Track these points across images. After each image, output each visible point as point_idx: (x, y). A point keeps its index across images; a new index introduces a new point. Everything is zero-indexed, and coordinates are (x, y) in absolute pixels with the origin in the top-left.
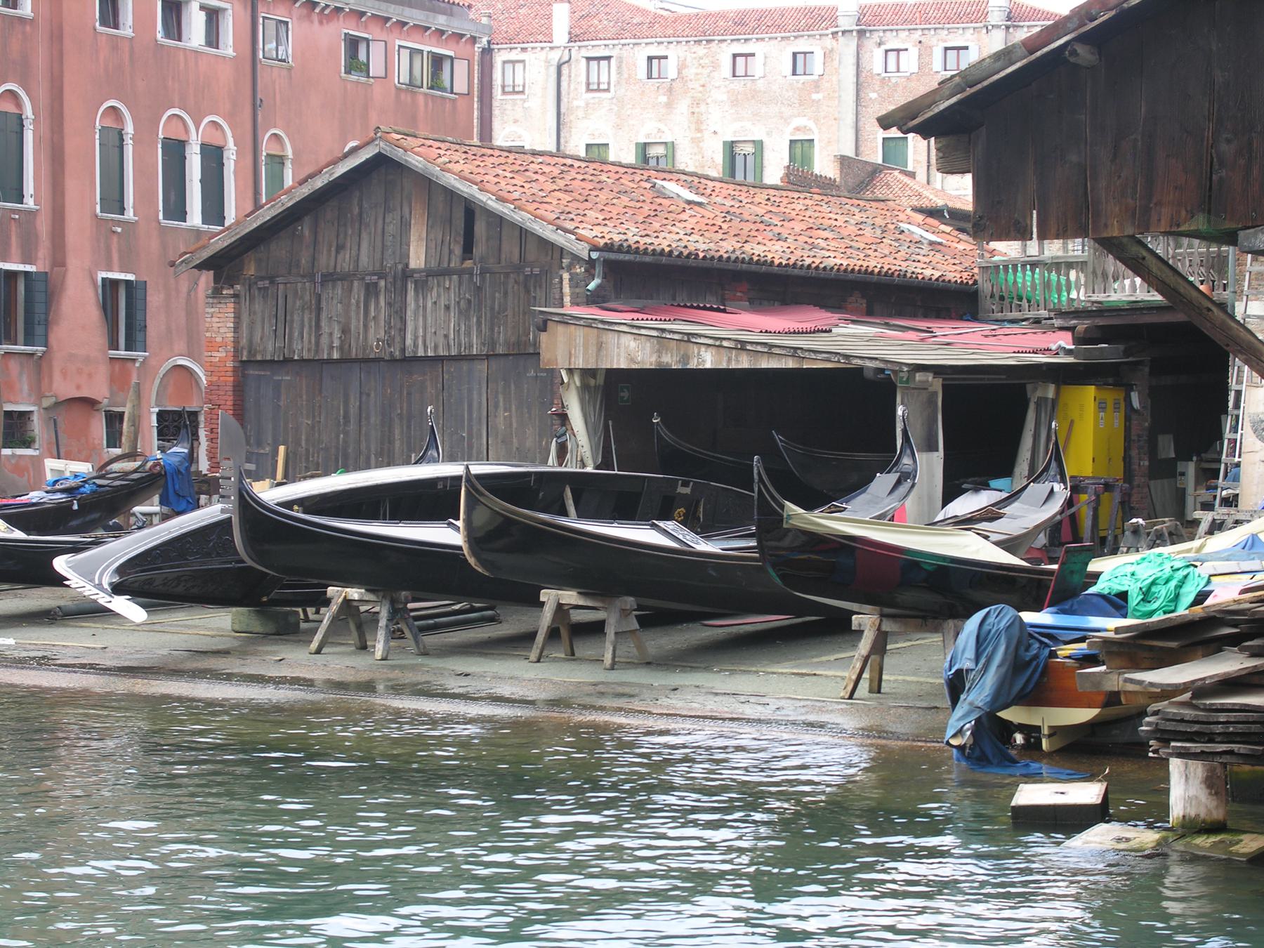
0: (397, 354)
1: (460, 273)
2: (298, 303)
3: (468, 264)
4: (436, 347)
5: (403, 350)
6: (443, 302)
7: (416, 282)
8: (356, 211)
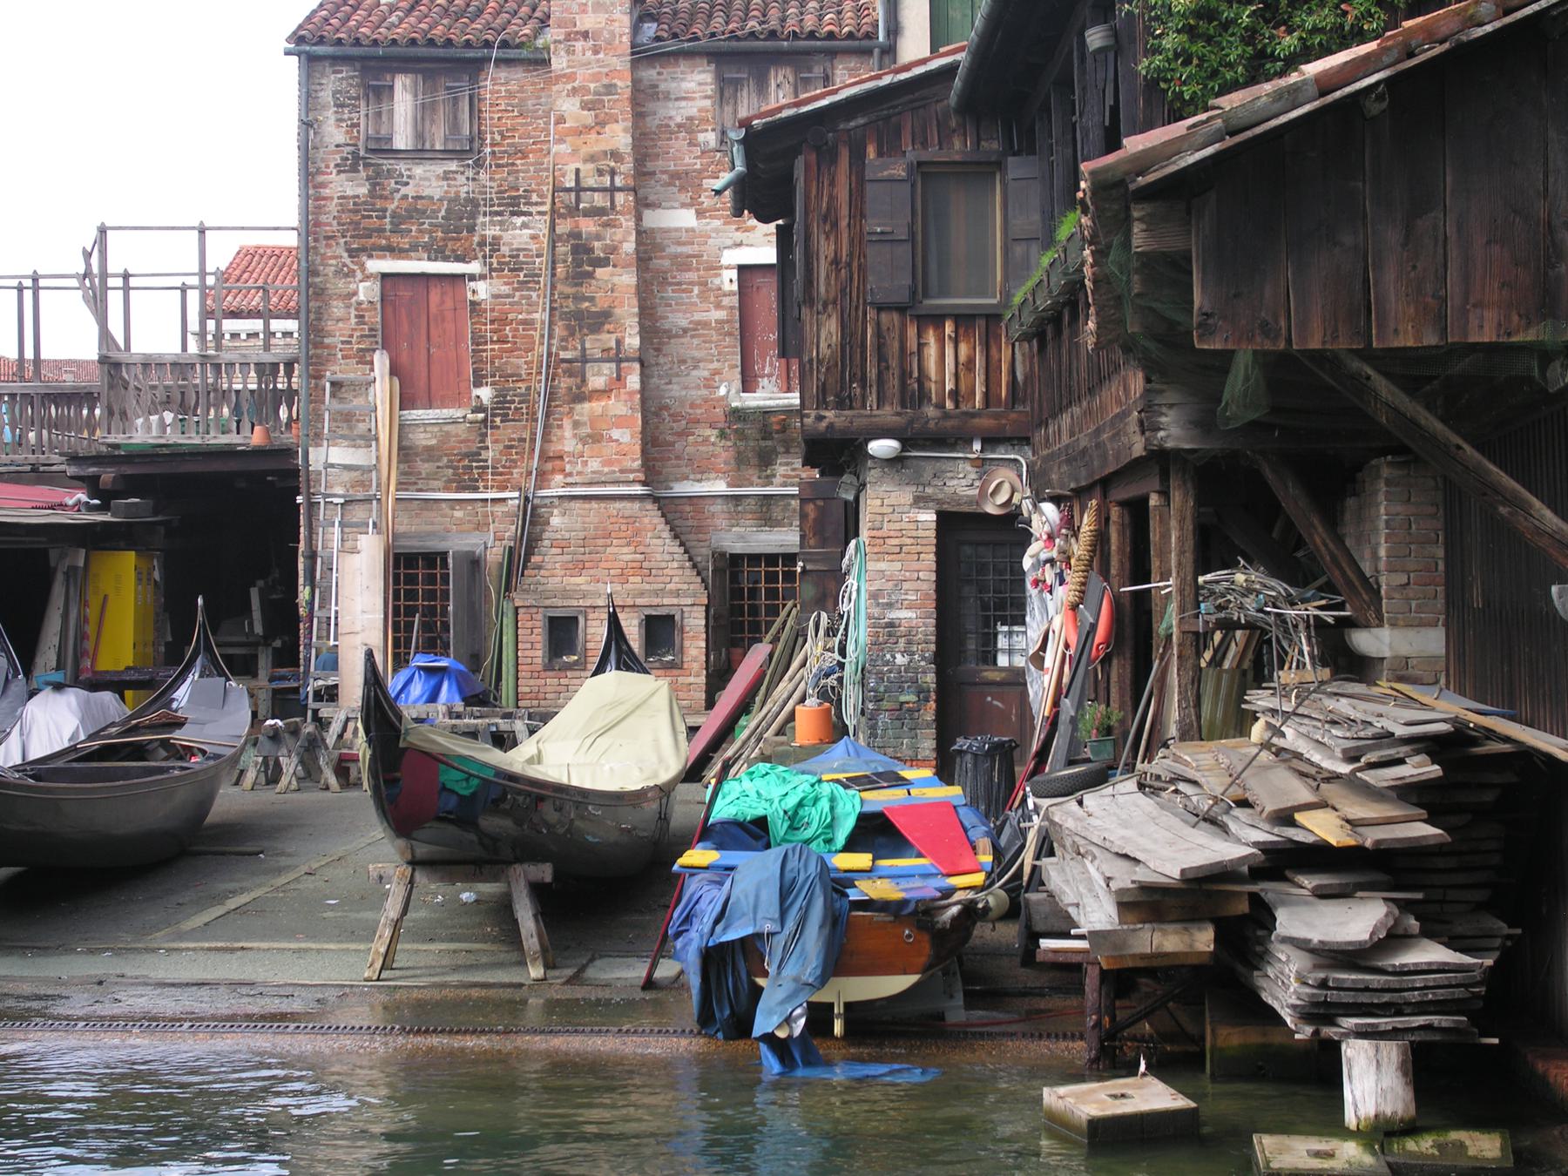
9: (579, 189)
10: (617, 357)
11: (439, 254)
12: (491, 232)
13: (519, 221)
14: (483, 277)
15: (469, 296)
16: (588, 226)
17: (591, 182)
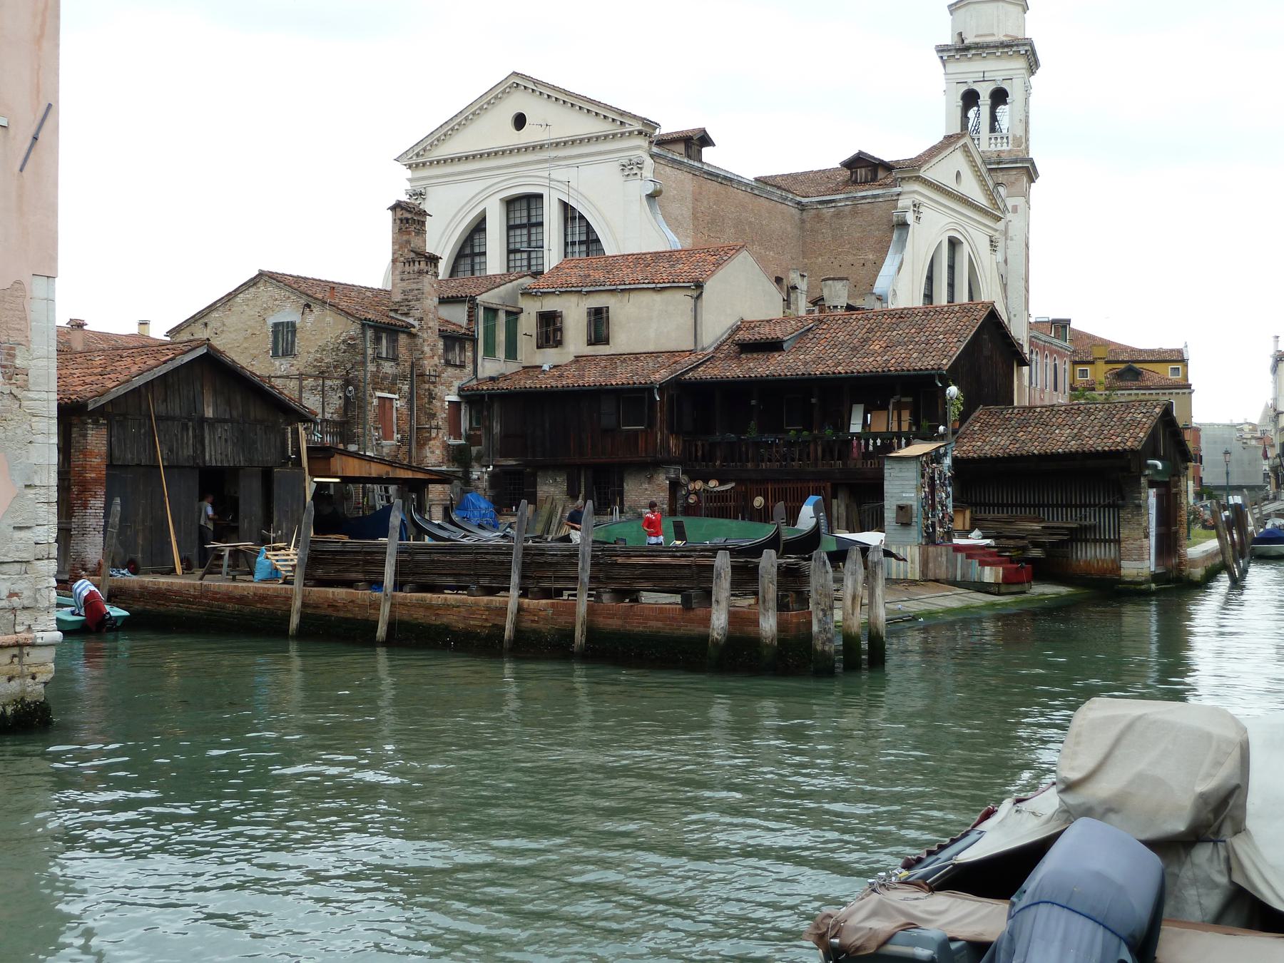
0: (201, 464)
4: (222, 461)
5: (204, 461)
9: (429, 375)
10: (438, 428)
15: (395, 406)
17: (432, 373)
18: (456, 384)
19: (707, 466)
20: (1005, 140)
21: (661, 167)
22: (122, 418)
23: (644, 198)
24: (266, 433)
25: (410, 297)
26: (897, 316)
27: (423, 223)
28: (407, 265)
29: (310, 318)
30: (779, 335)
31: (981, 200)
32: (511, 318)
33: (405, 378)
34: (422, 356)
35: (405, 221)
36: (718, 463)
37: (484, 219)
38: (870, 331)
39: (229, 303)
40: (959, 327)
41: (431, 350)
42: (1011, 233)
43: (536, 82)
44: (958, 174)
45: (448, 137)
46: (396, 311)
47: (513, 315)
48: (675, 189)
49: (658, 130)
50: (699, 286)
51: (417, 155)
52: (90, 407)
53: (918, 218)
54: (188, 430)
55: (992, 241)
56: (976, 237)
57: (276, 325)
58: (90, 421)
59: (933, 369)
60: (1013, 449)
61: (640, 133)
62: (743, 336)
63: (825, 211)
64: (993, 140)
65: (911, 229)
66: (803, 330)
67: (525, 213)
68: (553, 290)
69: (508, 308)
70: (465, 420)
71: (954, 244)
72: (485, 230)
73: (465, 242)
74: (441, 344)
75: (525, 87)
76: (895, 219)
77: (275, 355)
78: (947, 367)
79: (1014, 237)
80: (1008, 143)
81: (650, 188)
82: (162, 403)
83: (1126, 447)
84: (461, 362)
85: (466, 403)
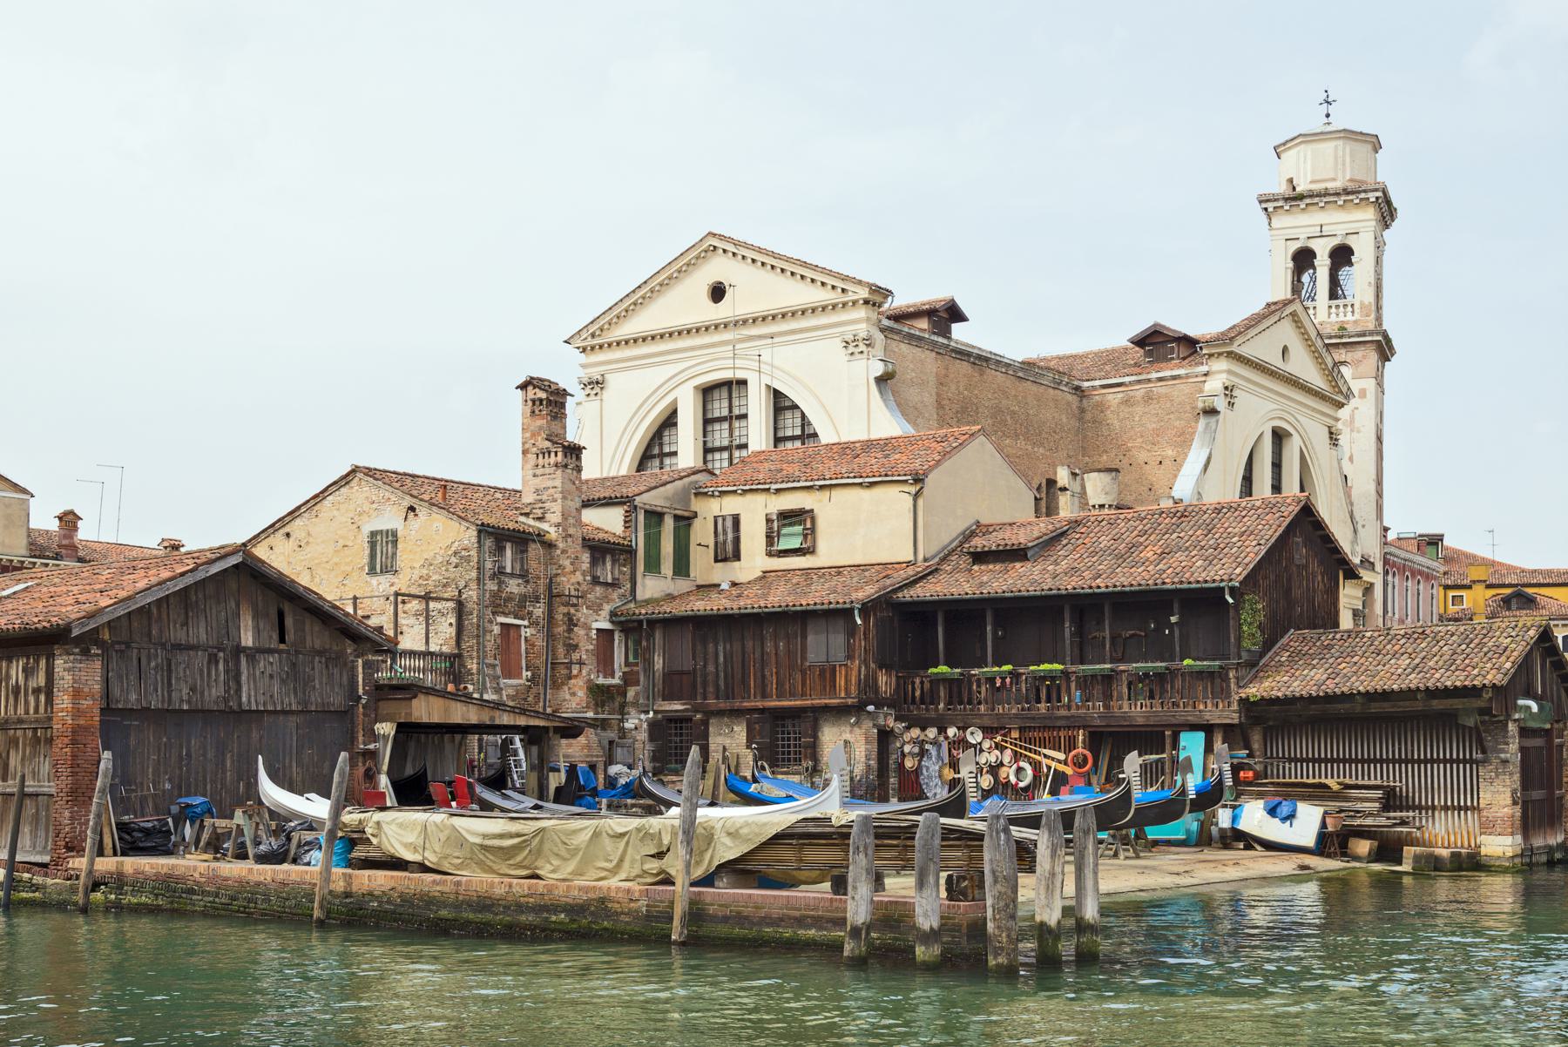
0: (235, 708)
1: (279, 652)
2: (153, 664)
3: (282, 646)
4: (264, 704)
5: (240, 704)
6: (269, 671)
7: (247, 656)
8: (194, 598)
9: (569, 596)
10: (581, 663)
11: (516, 617)
12: (531, 609)
13: (538, 605)
14: (529, 627)
15: (523, 634)
16: (572, 610)
17: (573, 593)
18: (607, 608)
19: (927, 710)
20: (1349, 309)
21: (894, 344)
22: (123, 647)
23: (872, 382)
24: (327, 667)
25: (544, 498)
26: (1178, 514)
27: (563, 405)
28: (541, 456)
29: (414, 523)
30: (1022, 541)
31: (1317, 380)
32: (682, 523)
33: (537, 599)
34: (559, 571)
35: (538, 403)
36: (941, 706)
37: (675, 412)
38: (1143, 533)
39: (316, 508)
40: (1260, 527)
41: (572, 564)
42: (1357, 424)
43: (737, 244)
44: (1285, 350)
45: (630, 313)
46: (527, 515)
47: (685, 522)
48: (913, 370)
49: (890, 299)
50: (918, 480)
51: (593, 335)
52: (75, 632)
53: (1231, 404)
54: (217, 663)
55: (1331, 433)
56: (1308, 427)
57: (373, 534)
58: (77, 650)
59: (1222, 580)
60: (1330, 687)
61: (866, 302)
62: (978, 543)
63: (1110, 397)
64: (1333, 310)
65: (1221, 417)
66: (1054, 534)
67: (725, 404)
68: (735, 488)
69: (679, 512)
70: (620, 653)
71: (1279, 436)
72: (675, 424)
73: (652, 439)
74: (586, 557)
75: (725, 251)
76: (1200, 405)
77: (372, 571)
78: (1241, 578)
79: (1362, 429)
80: (1353, 312)
81: (879, 369)
82: (182, 625)
83: (1485, 682)
84: (613, 579)
85: (621, 631)
